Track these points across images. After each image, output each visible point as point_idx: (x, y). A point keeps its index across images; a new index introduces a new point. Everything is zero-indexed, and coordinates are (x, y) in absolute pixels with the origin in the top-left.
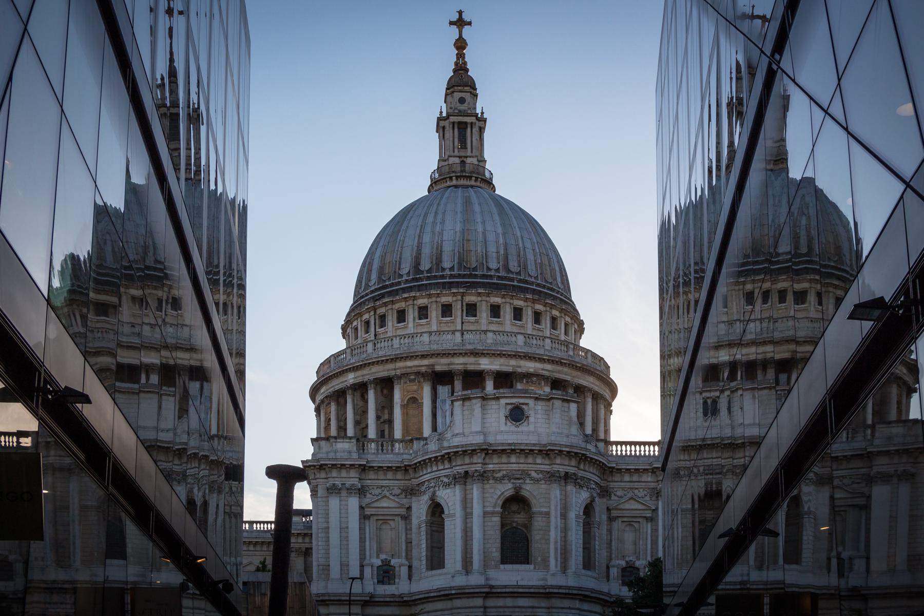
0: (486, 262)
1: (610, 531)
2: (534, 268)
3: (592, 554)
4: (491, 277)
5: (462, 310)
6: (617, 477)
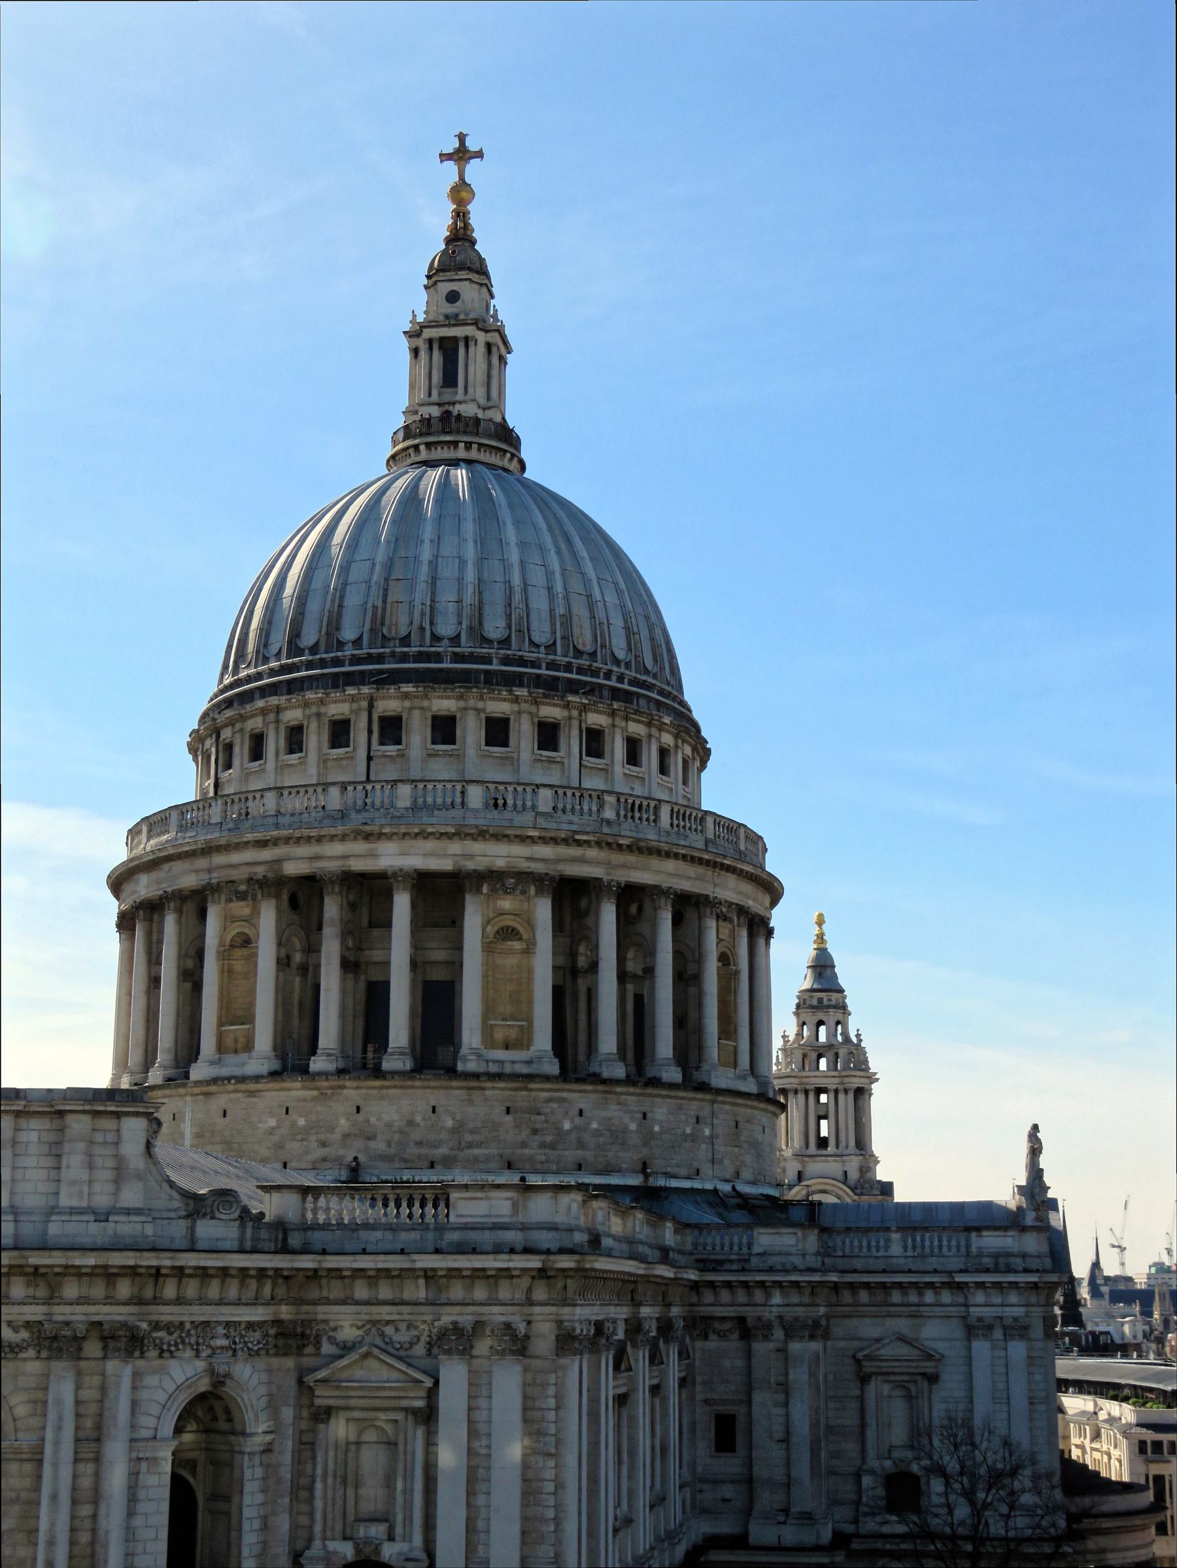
0: (432, 623)
1: (306, 1447)
2: (547, 627)
3: (234, 1534)
4: (438, 657)
5: (370, 732)
6: (335, 1290)
